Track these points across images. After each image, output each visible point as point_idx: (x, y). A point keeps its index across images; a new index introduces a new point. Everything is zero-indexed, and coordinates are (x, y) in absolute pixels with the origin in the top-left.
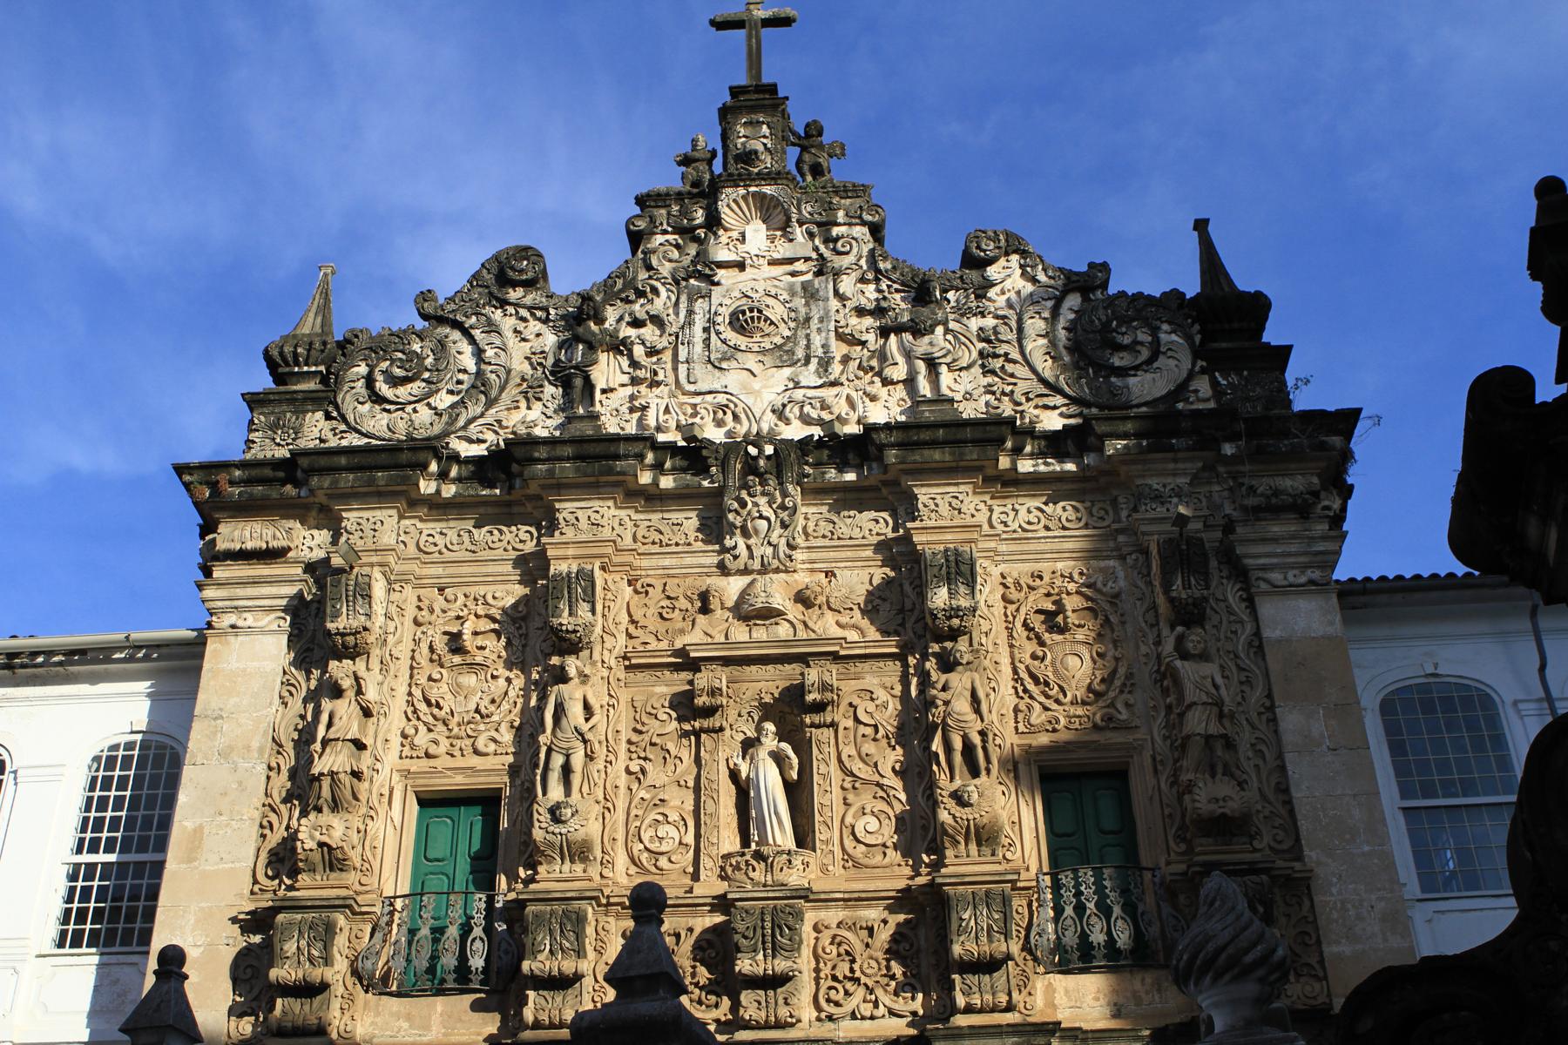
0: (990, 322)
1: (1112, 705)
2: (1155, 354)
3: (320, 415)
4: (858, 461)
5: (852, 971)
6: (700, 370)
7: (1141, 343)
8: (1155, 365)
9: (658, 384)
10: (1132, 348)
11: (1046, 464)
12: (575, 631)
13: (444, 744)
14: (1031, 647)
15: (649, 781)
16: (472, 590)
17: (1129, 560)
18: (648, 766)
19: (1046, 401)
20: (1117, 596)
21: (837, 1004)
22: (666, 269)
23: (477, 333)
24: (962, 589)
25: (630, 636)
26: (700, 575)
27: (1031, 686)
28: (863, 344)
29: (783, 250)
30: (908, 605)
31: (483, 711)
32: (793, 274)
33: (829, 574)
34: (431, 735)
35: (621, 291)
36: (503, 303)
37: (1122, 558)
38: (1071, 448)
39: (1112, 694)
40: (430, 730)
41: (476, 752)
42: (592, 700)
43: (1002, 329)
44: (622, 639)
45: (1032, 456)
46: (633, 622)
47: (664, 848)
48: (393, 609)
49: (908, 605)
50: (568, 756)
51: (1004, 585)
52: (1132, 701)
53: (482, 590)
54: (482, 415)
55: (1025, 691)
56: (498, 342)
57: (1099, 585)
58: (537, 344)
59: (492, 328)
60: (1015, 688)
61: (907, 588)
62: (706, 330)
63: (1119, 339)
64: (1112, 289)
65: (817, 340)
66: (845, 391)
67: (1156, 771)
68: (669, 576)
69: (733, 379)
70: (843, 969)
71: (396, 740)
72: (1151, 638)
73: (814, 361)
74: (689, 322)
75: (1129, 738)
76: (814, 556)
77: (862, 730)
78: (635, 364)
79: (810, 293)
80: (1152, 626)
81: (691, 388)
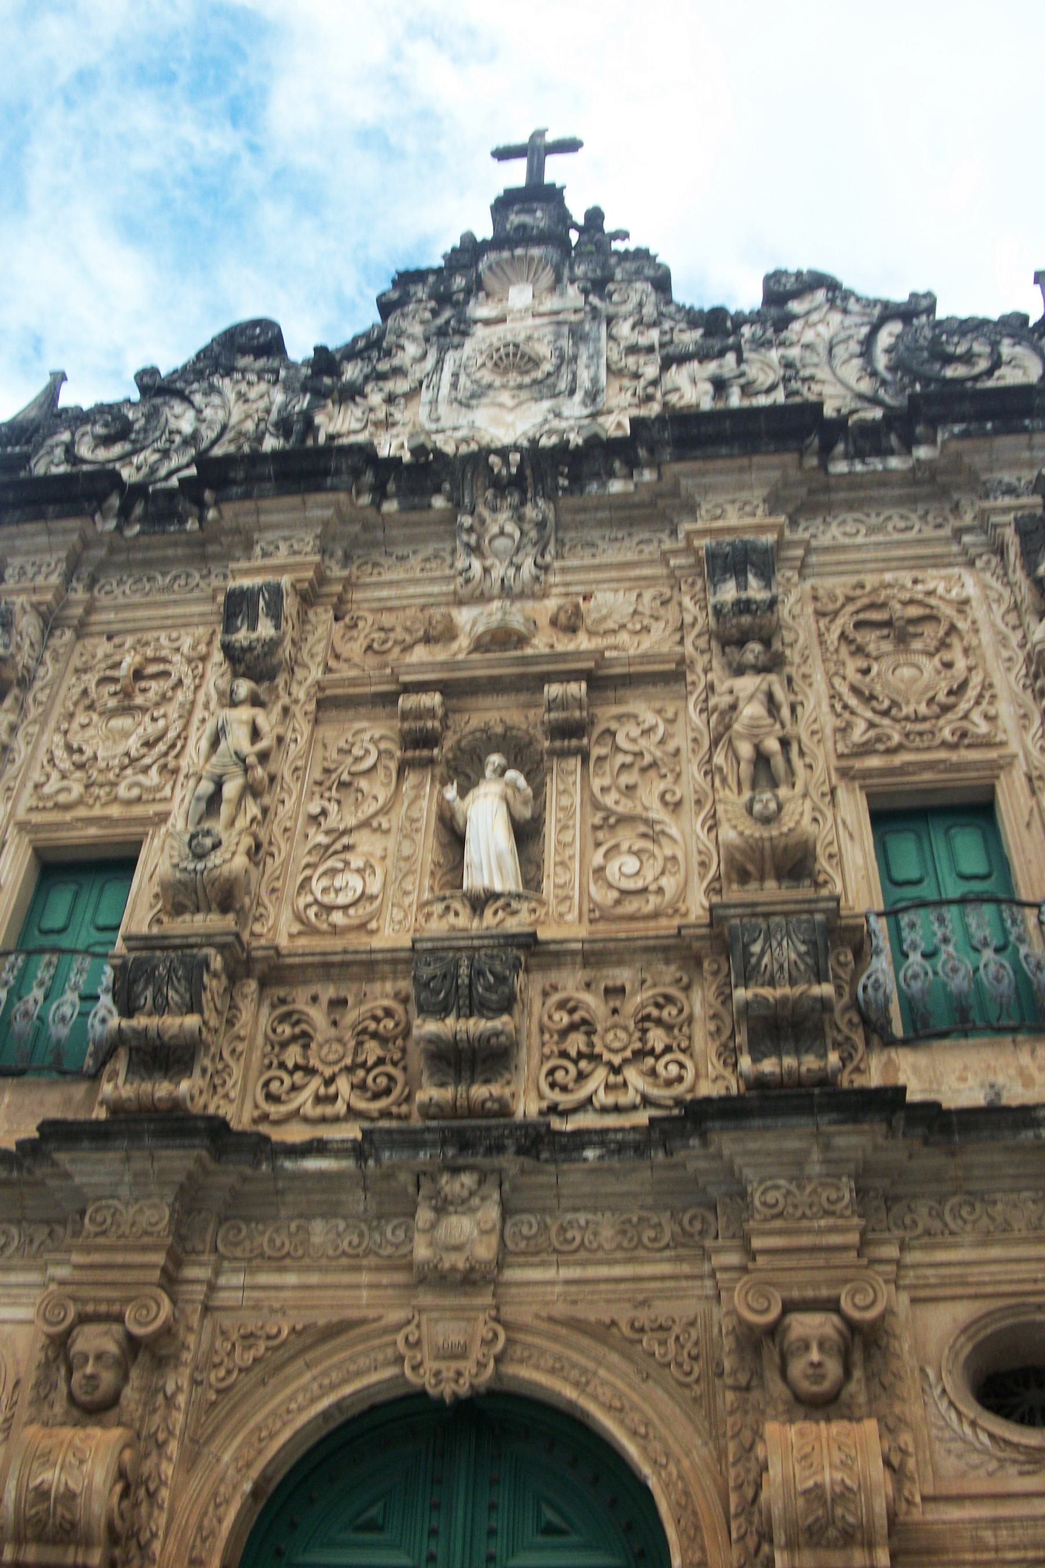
1: (966, 717)
2: (997, 363)
4: (625, 471)
5: (591, 1045)
6: (443, 409)
7: (979, 356)
8: (997, 374)
9: (394, 424)
10: (968, 358)
11: (864, 463)
12: (250, 648)
13: (77, 789)
14: (852, 666)
15: (332, 821)
16: (149, 636)
17: (979, 564)
18: (333, 808)
20: (966, 602)
21: (564, 1089)
23: (198, 399)
24: (753, 581)
25: (328, 669)
26: (423, 608)
27: (853, 701)
28: (636, 376)
29: (551, 303)
30: (688, 619)
31: (133, 753)
32: (559, 323)
34: (65, 783)
35: (361, 351)
36: (228, 371)
37: (971, 563)
38: (894, 440)
39: (963, 706)
40: (64, 777)
41: (116, 799)
43: (808, 354)
44: (316, 673)
45: (847, 456)
46: (337, 657)
47: (342, 899)
48: (48, 656)
49: (688, 619)
50: (219, 786)
51: (815, 598)
52: (992, 712)
53: (155, 634)
55: (845, 707)
56: (216, 399)
57: (941, 590)
58: (262, 404)
59: (212, 389)
60: (833, 706)
61: (687, 601)
62: (456, 375)
63: (950, 349)
64: (941, 314)
65: (584, 377)
67: (1033, 792)
68: (390, 609)
70: (576, 1042)
72: (1015, 638)
75: (992, 754)
76: (569, 578)
77: (620, 759)
78: (371, 410)
79: (578, 335)
80: (1014, 628)
81: (433, 427)
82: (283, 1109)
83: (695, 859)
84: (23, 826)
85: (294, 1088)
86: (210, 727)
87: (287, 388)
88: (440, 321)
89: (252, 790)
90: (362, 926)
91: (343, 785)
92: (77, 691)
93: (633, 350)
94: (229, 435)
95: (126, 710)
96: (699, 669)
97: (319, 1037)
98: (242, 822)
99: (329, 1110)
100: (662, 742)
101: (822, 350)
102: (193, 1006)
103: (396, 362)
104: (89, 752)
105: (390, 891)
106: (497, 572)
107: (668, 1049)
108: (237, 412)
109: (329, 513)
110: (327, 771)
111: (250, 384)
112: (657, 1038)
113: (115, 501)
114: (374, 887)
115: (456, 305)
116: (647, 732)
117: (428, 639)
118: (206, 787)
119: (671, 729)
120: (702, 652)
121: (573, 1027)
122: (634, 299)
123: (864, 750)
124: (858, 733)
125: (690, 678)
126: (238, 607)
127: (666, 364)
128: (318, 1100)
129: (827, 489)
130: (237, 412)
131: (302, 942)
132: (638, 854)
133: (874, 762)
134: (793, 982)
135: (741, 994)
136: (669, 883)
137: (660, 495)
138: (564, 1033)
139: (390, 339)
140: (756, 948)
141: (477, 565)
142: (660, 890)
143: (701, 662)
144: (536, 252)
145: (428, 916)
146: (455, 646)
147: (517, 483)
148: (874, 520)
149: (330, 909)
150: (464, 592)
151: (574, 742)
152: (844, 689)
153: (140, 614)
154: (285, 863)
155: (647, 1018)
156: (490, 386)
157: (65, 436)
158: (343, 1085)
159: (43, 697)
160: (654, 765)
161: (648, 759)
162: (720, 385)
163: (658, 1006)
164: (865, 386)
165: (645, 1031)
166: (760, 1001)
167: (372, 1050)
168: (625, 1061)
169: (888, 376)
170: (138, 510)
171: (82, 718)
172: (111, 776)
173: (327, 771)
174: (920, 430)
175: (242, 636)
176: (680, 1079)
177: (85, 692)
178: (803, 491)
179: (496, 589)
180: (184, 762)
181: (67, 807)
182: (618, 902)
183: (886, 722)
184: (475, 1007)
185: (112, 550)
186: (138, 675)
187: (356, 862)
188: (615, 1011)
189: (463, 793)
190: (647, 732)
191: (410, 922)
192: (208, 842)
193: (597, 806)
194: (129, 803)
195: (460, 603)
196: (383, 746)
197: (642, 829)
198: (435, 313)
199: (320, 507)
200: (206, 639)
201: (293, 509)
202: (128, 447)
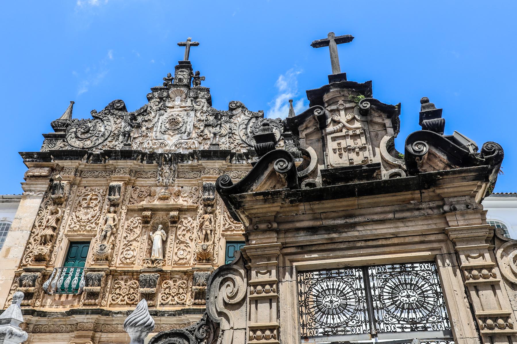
0: (233, 125)
3: (61, 140)
13: (78, 227)
15: (128, 239)
19: (242, 145)
21: (164, 300)
22: (155, 108)
24: (211, 193)
25: (130, 201)
26: (150, 187)
27: (227, 219)
28: (200, 129)
29: (184, 104)
32: (185, 110)
33: (182, 187)
38: (245, 158)
42: (116, 217)
46: (132, 198)
47: (129, 257)
50: (107, 233)
54: (102, 143)
56: (109, 124)
58: (119, 125)
59: (109, 120)
62: (161, 123)
65: (188, 127)
66: (193, 141)
69: (166, 136)
70: (167, 291)
71: (67, 226)
73: (187, 133)
74: (158, 121)
82: (115, 302)
83: (193, 253)
84: (66, 235)
85: (117, 298)
86: (105, 218)
87: (125, 122)
88: (160, 106)
89: (112, 234)
90: (132, 263)
91: (131, 230)
92: (78, 201)
93: (199, 120)
94: (112, 134)
95: (88, 207)
96: (200, 208)
97: (122, 288)
98: (111, 241)
99: (123, 303)
100: (191, 225)
101: (238, 125)
102: (99, 285)
103: (149, 118)
104: (80, 218)
105: (138, 255)
106: (165, 180)
107: (183, 293)
108: (114, 126)
109: (132, 164)
110: (128, 226)
111: (117, 118)
112: (181, 291)
113: (86, 156)
114: (135, 255)
115: (164, 101)
116: (189, 222)
117: (150, 195)
118: (104, 233)
119: (194, 222)
120: (202, 204)
121: (167, 288)
122: (202, 105)
123: (227, 230)
124: (226, 227)
125: (198, 210)
126: (112, 190)
127: (206, 126)
128: (122, 301)
129: (231, 166)
130: (114, 126)
131: (121, 265)
132: (183, 250)
133: (229, 233)
134: (203, 285)
135: (194, 287)
136: (188, 257)
137: (199, 165)
138: (165, 289)
139: (149, 109)
140: (197, 279)
141: (161, 178)
142: (186, 259)
143: (201, 207)
144: (182, 89)
145: (144, 263)
146: (155, 197)
147: (170, 160)
148: (240, 173)
149: (126, 259)
150: (158, 184)
151: (175, 225)
152: (226, 215)
153: (91, 182)
154: (119, 248)
155: (180, 286)
156: (168, 129)
157: (75, 130)
158: (126, 297)
159: (70, 203)
160: (189, 230)
161: (188, 228)
162: (215, 134)
163: (182, 284)
164: (244, 138)
165: (179, 289)
166: (196, 289)
167: (132, 291)
168: (175, 295)
169: (249, 134)
170: (91, 158)
171: (78, 209)
172: (85, 224)
173: (128, 226)
174: (250, 156)
175: (112, 197)
176: (184, 299)
177: (80, 202)
178: (226, 166)
179: (164, 184)
180: (100, 221)
181: (75, 231)
182: (179, 261)
183: (232, 224)
184: (150, 286)
185: (85, 165)
186: (91, 199)
187: (132, 249)
188: (175, 285)
189: (153, 233)
190: (189, 222)
191: (141, 263)
192: (104, 247)
193: (178, 239)
194: (88, 231)
195: (158, 186)
196: (140, 221)
197: (185, 244)
198: (159, 103)
199: (130, 163)
200: (105, 190)
201: (124, 162)
202: (89, 135)
